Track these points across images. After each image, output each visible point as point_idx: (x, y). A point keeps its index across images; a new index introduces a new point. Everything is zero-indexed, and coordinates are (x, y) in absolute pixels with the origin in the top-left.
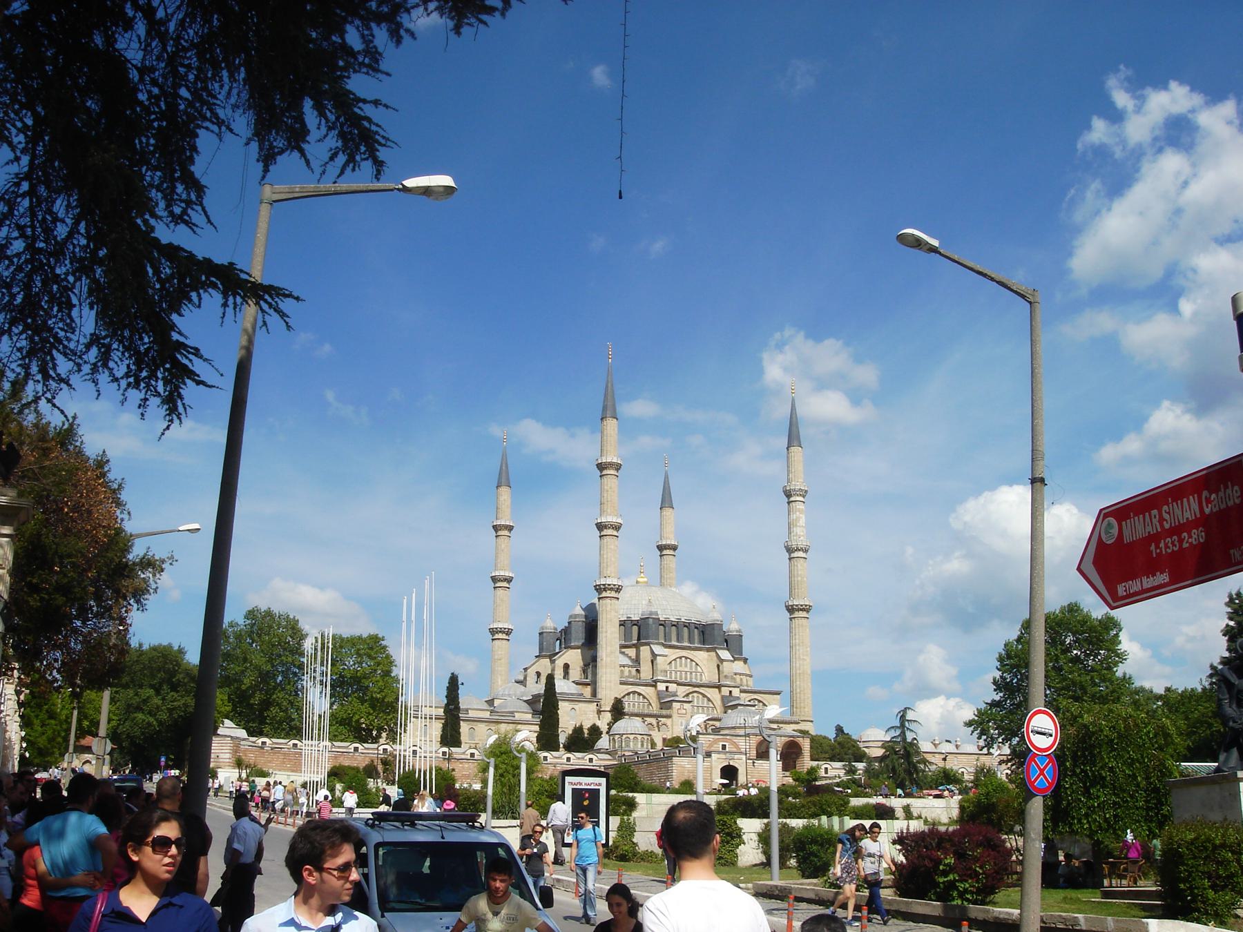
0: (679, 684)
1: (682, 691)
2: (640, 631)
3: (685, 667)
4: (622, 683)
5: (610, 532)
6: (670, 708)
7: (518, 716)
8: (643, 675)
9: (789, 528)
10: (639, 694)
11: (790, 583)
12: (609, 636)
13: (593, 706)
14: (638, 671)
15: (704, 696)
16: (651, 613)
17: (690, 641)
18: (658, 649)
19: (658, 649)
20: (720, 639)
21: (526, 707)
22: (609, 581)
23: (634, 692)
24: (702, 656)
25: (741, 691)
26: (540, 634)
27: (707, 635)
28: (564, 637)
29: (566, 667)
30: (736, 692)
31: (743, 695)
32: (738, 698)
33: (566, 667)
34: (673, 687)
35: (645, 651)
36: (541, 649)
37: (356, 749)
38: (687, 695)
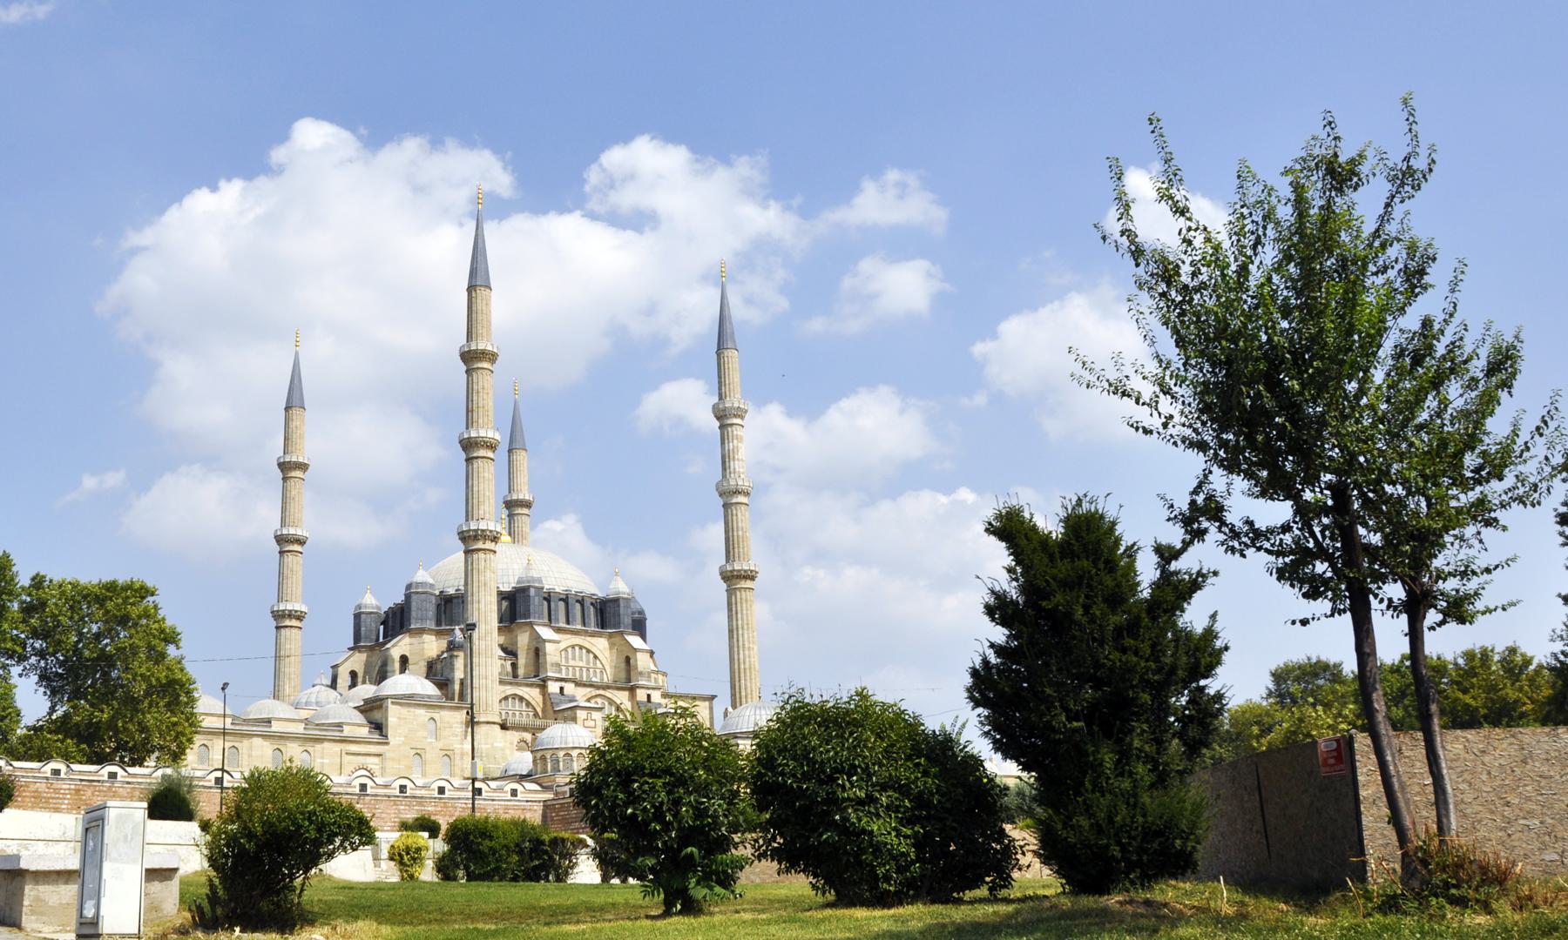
0: (578, 684)
1: (581, 694)
2: (516, 606)
3: (580, 661)
4: (502, 682)
5: (482, 453)
6: (574, 719)
7: (348, 731)
8: (521, 671)
9: (724, 463)
10: (521, 699)
11: (727, 540)
12: (485, 611)
13: (462, 716)
14: (514, 666)
15: (611, 702)
16: (534, 579)
17: (584, 624)
18: (545, 632)
19: (545, 632)
20: (627, 620)
21: (359, 718)
22: (483, 526)
23: (514, 696)
24: (600, 645)
25: (665, 696)
26: (357, 616)
27: (607, 614)
28: (397, 621)
29: (404, 660)
30: (656, 697)
31: (664, 701)
32: (660, 705)
33: (404, 660)
34: (569, 688)
35: (523, 640)
36: (357, 637)
37: (113, 775)
38: (588, 700)
